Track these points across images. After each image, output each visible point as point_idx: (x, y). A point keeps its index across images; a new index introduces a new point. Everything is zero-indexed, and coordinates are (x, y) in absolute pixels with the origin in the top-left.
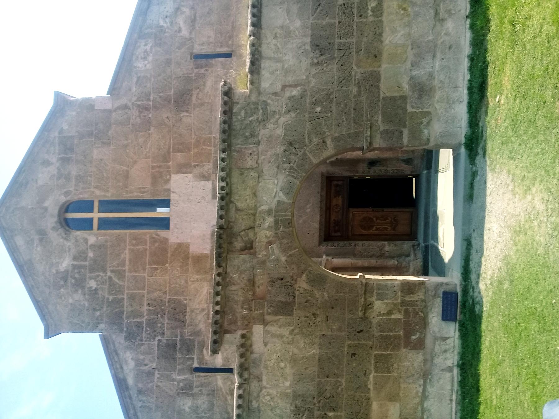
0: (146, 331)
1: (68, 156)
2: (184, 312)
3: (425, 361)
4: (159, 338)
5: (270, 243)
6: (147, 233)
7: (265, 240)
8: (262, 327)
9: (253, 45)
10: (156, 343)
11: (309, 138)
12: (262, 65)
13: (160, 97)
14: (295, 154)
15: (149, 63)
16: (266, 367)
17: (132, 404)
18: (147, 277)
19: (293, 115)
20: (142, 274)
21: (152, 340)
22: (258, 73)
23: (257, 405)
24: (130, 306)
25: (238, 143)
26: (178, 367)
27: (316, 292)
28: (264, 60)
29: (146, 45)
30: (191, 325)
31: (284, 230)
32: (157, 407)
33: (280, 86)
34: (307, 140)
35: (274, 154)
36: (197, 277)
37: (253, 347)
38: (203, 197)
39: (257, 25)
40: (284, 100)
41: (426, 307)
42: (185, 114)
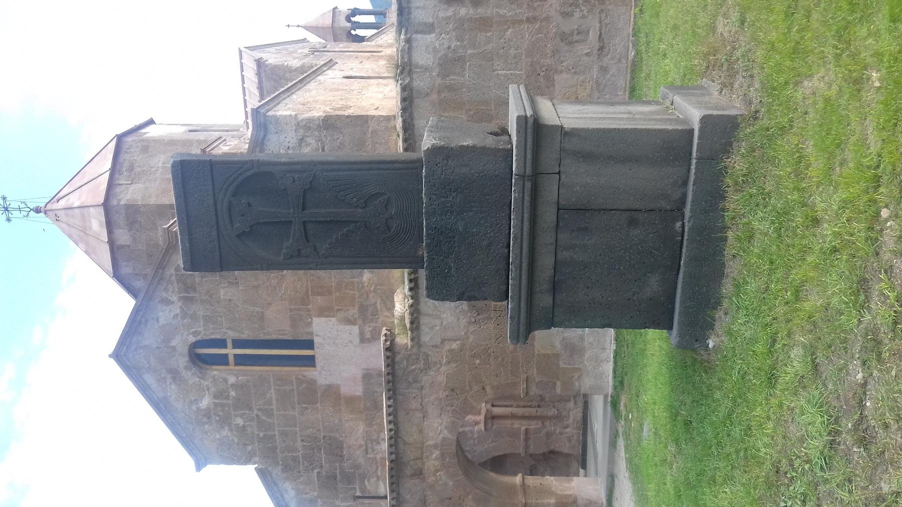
0: (303, 464)
1: (191, 295)
2: (341, 448)
5: (438, 471)
7: (432, 468)
10: (316, 475)
12: (421, 322)
18: (297, 416)
19: (454, 365)
20: (292, 413)
21: (310, 472)
26: (340, 495)
28: (423, 317)
31: (450, 461)
36: (351, 416)
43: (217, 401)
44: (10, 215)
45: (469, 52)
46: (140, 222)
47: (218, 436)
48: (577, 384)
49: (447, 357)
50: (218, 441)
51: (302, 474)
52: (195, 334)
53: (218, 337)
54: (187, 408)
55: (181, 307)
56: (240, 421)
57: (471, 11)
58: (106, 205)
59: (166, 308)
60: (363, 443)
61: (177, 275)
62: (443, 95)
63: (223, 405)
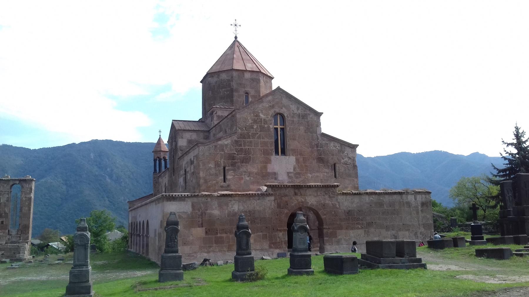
0: (239, 148)
4: (236, 153)
5: (297, 200)
6: (273, 148)
7: (298, 199)
8: (274, 199)
9: (350, 193)
11: (326, 211)
14: (321, 206)
16: (262, 201)
19: (332, 206)
20: (259, 146)
25: (324, 190)
27: (284, 215)
29: (338, 146)
30: (241, 166)
32: (210, 153)
34: (325, 210)
35: (321, 200)
38: (288, 169)
40: (335, 203)
41: (281, 248)
42: (316, 161)
43: (263, 120)
46: (253, 83)
47: (249, 118)
48: (328, 244)
49: (334, 203)
50: (246, 118)
53: (287, 124)
54: (260, 109)
55: (296, 113)
56: (255, 127)
57: (420, 210)
58: (260, 72)
60: (249, 171)
61: (307, 114)
62: (402, 202)
63: (261, 122)
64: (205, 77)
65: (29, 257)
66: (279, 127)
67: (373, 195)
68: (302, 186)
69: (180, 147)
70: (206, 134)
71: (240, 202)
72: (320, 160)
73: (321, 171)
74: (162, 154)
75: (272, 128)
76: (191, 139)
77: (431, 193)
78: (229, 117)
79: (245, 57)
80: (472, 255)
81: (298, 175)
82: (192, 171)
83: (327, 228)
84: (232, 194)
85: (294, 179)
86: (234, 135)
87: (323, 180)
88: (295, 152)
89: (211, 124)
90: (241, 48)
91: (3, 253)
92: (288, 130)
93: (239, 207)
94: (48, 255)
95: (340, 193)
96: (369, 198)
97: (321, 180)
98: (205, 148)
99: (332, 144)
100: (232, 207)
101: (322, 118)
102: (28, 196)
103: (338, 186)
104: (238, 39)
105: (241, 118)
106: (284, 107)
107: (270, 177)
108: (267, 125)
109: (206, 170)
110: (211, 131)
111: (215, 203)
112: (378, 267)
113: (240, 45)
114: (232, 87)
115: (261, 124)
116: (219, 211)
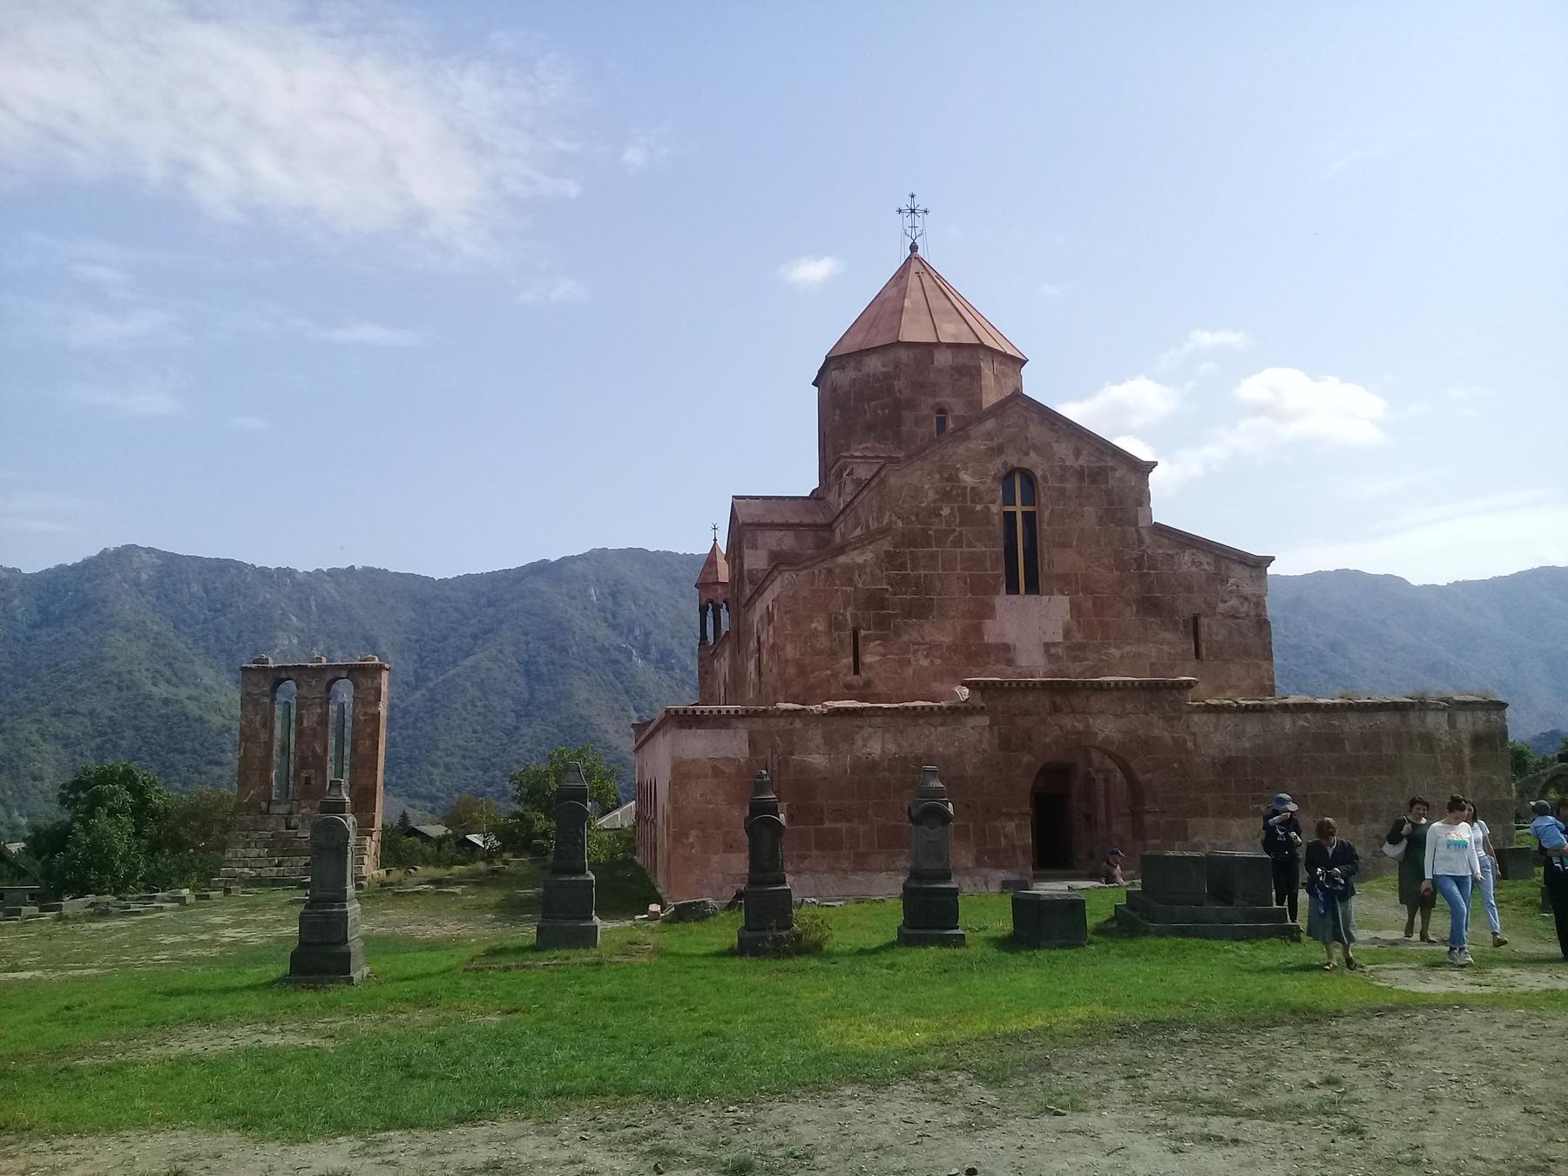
3: (967, 869)
4: (890, 590)
5: (1061, 727)
6: (1001, 571)
9: (1229, 705)
12: (1212, 715)
13: (1152, 581)
15: (1189, 567)
17: (819, 562)
19: (1171, 743)
20: (959, 567)
22: (1206, 712)
23: (920, 722)
24: (923, 554)
26: (859, 613)
29: (1208, 564)
33: (1194, 731)
34: (1151, 756)
37: (971, 717)
39: (1247, 709)
42: (1134, 611)
43: (969, 490)
44: (906, 214)
45: (1439, 756)
47: (926, 487)
49: (1179, 737)
50: (920, 485)
51: (885, 572)
52: (1045, 478)
53: (1043, 500)
54: (961, 458)
56: (946, 512)
57: (1467, 758)
58: (982, 346)
59: (1071, 451)
60: (927, 640)
61: (1106, 467)
62: (1405, 736)
63: (964, 495)
64: (822, 371)
65: (375, 872)
66: (1019, 509)
67: (1305, 713)
68: (1075, 683)
69: (750, 571)
70: (825, 534)
71: (888, 731)
72: (1150, 606)
73: (1153, 639)
74: (720, 591)
75: (996, 511)
76: (778, 549)
77: (1508, 705)
78: (873, 484)
79: (937, 302)
80: (1530, 903)
81: (1076, 650)
82: (771, 641)
83: (1157, 810)
84: (863, 709)
85: (1069, 664)
86: (884, 538)
87: (1158, 666)
88: (1066, 583)
89: (839, 504)
90: (926, 278)
91: (308, 861)
92: (1046, 520)
93: (887, 746)
94: (415, 869)
95: (1198, 706)
96: (1294, 722)
97: (1152, 665)
98: (800, 578)
99: (1187, 557)
100: (865, 746)
101: (1154, 478)
102: (371, 710)
103: (1189, 685)
104: (920, 253)
105: (903, 487)
106: (1034, 450)
107: (992, 657)
108: (982, 506)
109: (803, 638)
110: (836, 525)
111: (816, 735)
112: (1146, 933)
113: (923, 266)
114: (898, 395)
115: (966, 503)
116: (827, 757)
